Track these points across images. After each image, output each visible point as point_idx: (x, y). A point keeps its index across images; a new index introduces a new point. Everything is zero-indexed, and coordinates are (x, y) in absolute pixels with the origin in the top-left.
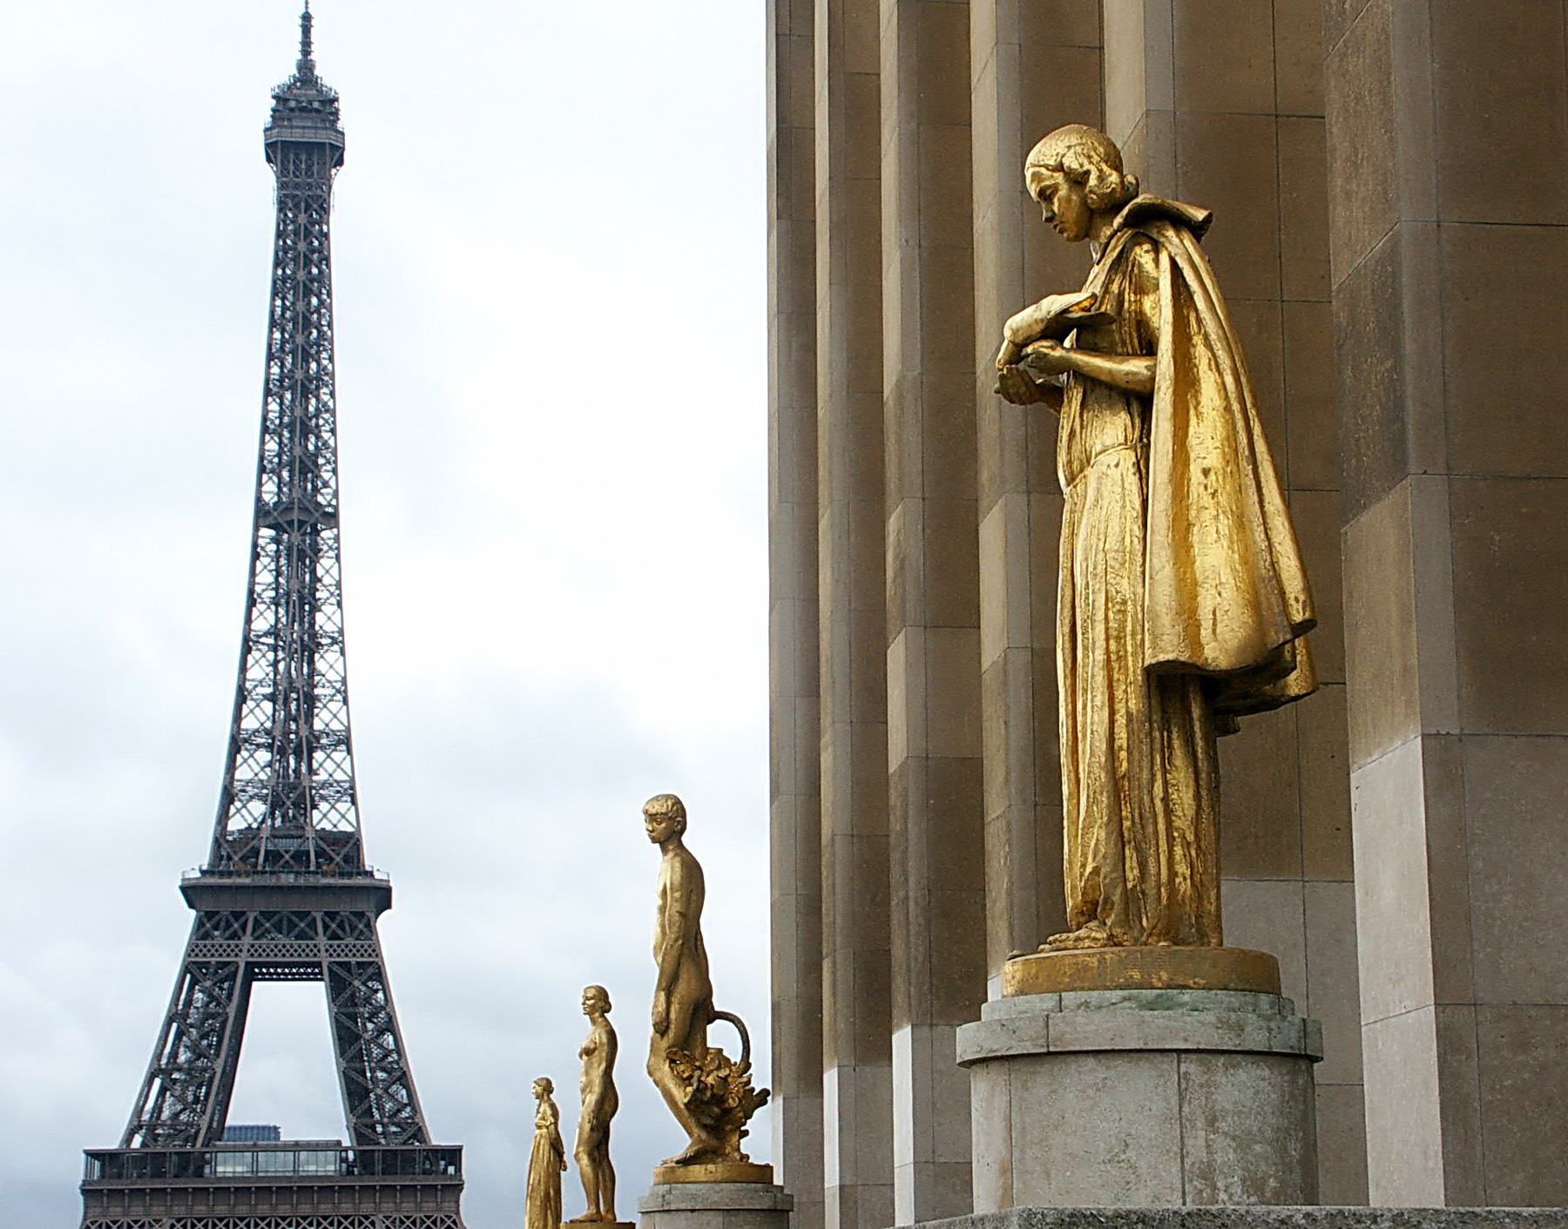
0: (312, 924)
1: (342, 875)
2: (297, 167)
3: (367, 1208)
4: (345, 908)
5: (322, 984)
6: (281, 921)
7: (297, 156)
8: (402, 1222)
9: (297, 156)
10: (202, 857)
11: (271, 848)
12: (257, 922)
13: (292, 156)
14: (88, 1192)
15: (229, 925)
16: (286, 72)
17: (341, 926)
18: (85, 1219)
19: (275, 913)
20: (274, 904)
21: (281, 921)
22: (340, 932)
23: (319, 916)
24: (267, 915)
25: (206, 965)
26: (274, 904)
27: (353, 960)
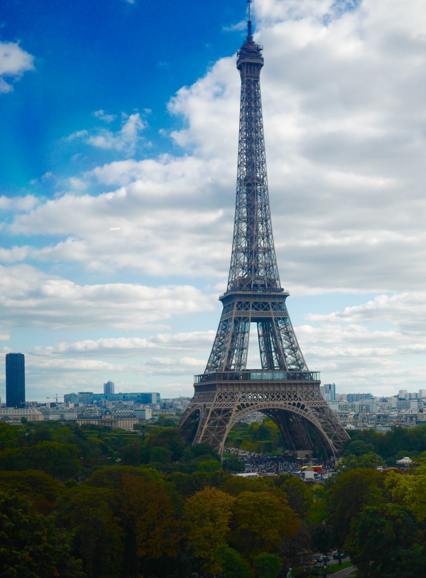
0: (268, 306)
2: (250, 71)
3: (294, 389)
4: (277, 301)
6: (259, 305)
7: (250, 67)
9: (250, 67)
12: (253, 306)
13: (249, 67)
15: (245, 306)
16: (245, 39)
19: (258, 302)
20: (257, 300)
21: (259, 305)
23: (270, 304)
24: (256, 303)
25: (239, 318)
26: (257, 300)
27: (281, 317)
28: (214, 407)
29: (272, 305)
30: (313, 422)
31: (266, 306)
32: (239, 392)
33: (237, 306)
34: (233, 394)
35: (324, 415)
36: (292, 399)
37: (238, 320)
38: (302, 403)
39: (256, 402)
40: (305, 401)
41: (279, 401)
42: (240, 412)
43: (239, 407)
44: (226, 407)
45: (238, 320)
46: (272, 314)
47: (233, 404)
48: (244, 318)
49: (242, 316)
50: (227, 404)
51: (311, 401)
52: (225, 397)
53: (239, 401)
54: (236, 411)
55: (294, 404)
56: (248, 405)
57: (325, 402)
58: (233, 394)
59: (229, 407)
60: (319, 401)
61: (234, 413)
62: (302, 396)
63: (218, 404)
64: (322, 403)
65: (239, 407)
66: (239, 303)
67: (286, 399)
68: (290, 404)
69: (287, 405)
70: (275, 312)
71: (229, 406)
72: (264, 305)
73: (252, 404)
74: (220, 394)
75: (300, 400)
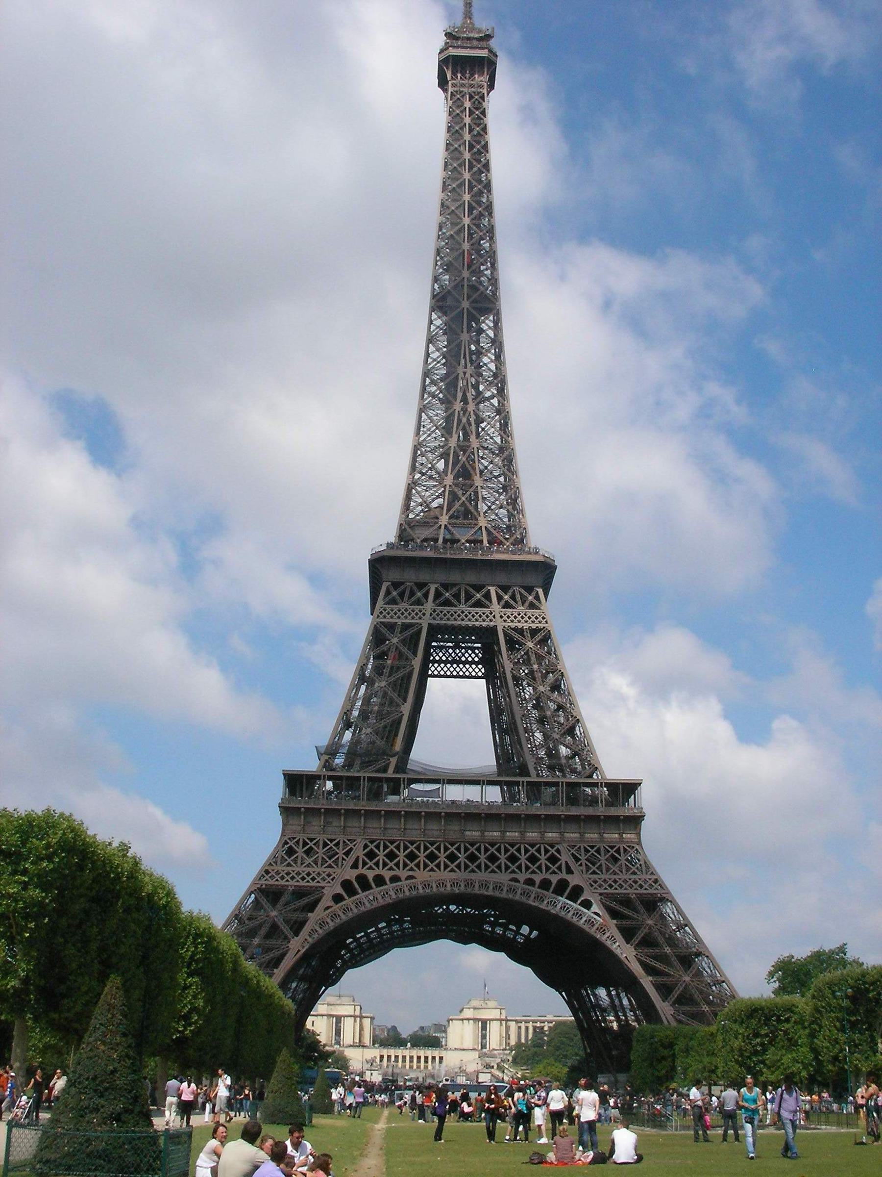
0: (488, 596)
1: (513, 553)
3: (551, 835)
5: (484, 680)
8: (587, 851)
10: (390, 535)
11: (448, 537)
12: (438, 595)
14: (286, 811)
15: (412, 594)
17: (513, 597)
18: (283, 835)
19: (455, 585)
20: (455, 577)
22: (512, 602)
24: (446, 587)
25: (391, 627)
27: (526, 626)
28: (263, 881)
29: (500, 591)
30: (608, 943)
31: (478, 596)
32: (359, 840)
33: (388, 592)
34: (337, 845)
35: (650, 922)
36: (540, 868)
37: (384, 630)
38: (574, 880)
39: (411, 873)
40: (586, 876)
41: (493, 871)
42: (348, 901)
43: (347, 885)
44: (303, 883)
45: (384, 630)
46: (498, 617)
47: (329, 875)
48: (406, 627)
49: (399, 622)
50: (308, 874)
51: (607, 877)
52: (308, 852)
53: (355, 866)
54: (337, 898)
55: (545, 884)
56: (380, 881)
57: (656, 881)
58: (337, 845)
59: (312, 884)
60: (633, 877)
61: (326, 901)
62: (577, 859)
63: (278, 873)
64: (645, 881)
65: (347, 885)
66: (396, 585)
67: (519, 868)
68: (530, 882)
69: (521, 886)
70: (509, 611)
71: (313, 879)
72: (471, 590)
73: (395, 879)
74: (291, 843)
75: (569, 871)
